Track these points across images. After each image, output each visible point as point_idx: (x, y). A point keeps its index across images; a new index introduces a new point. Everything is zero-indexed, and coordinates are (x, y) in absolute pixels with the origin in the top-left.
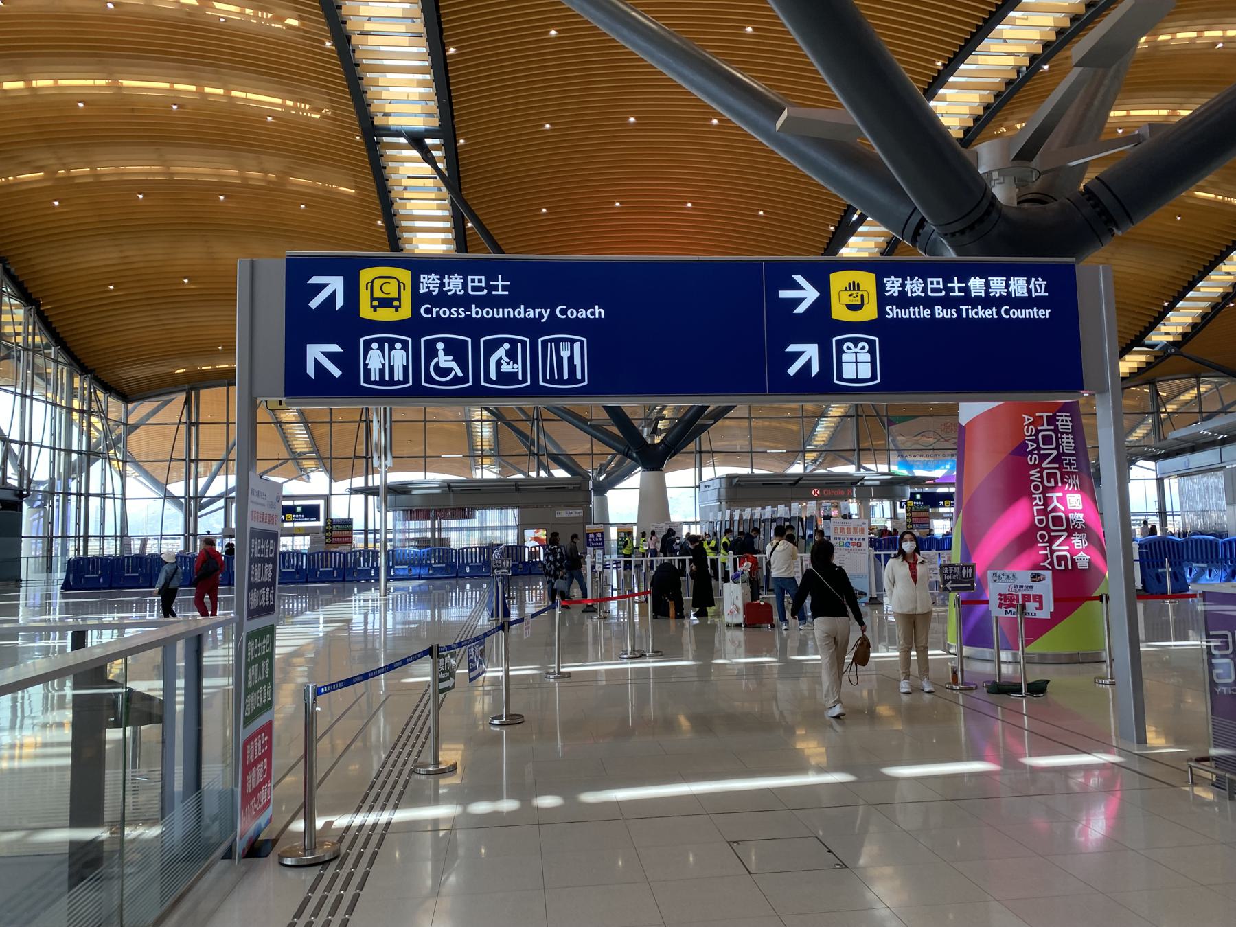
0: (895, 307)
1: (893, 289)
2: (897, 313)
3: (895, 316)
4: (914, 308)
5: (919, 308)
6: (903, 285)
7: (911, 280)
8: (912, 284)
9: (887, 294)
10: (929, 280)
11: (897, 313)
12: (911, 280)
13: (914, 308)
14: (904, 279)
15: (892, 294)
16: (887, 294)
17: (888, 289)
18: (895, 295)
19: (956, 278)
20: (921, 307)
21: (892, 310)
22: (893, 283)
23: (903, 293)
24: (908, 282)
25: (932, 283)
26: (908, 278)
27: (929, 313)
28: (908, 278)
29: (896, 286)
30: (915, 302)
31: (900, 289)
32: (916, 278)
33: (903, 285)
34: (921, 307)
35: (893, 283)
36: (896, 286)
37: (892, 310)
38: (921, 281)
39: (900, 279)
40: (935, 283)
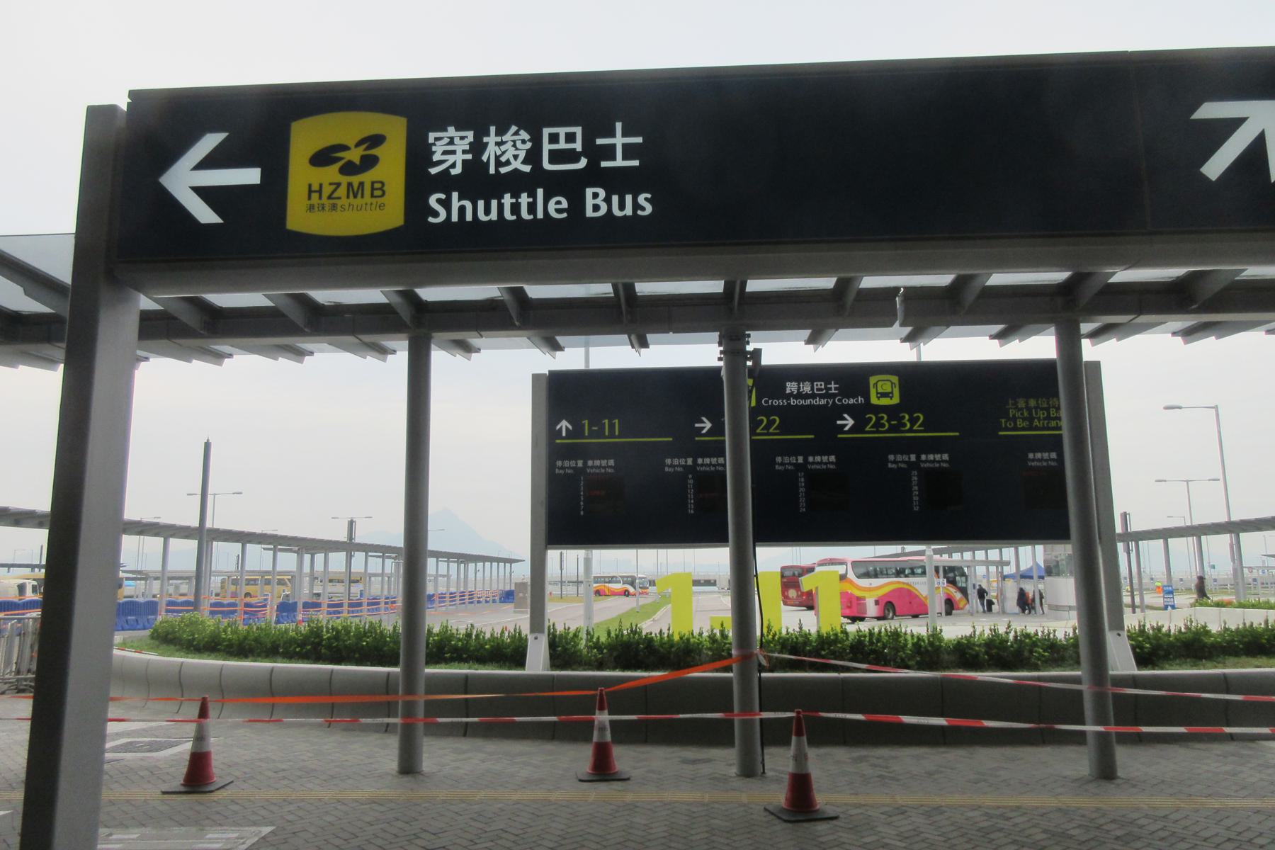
0: (455, 195)
1: (451, 159)
2: (462, 210)
3: (455, 218)
4: (516, 195)
5: (533, 195)
6: (477, 147)
7: (500, 132)
8: (499, 144)
9: (433, 171)
10: (546, 132)
11: (462, 210)
12: (500, 132)
13: (516, 195)
14: (481, 132)
15: (446, 171)
16: (433, 171)
17: (436, 158)
18: (454, 172)
19: (619, 126)
20: (540, 192)
21: (446, 204)
22: (451, 142)
23: (475, 167)
24: (491, 139)
25: (554, 138)
26: (493, 129)
27: (565, 204)
28: (493, 129)
29: (459, 149)
30: (516, 183)
31: (469, 157)
32: (514, 128)
33: (477, 147)
34: (540, 192)
35: (451, 142)
36: (459, 149)
37: (446, 204)
38: (524, 135)
39: (470, 135)
40: (562, 138)
